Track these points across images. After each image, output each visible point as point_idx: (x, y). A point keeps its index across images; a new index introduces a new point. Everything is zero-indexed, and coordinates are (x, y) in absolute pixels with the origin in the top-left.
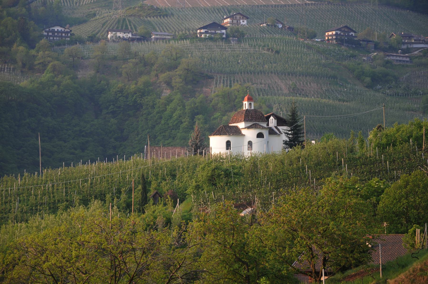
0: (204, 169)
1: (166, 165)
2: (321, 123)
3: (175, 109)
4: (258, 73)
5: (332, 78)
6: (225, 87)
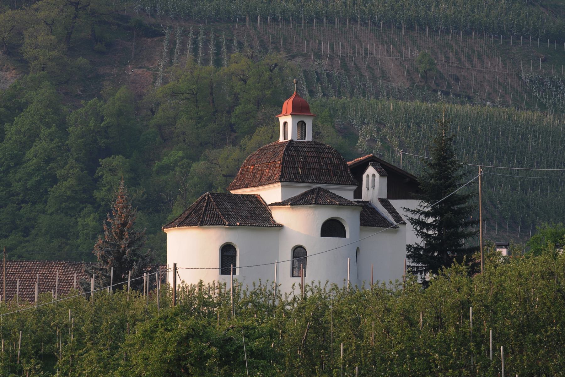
0: (152, 338)
1: (22, 322)
2: (514, 188)
3: (32, 137)
4: (310, 21)
5: (552, 42)
6: (199, 66)
